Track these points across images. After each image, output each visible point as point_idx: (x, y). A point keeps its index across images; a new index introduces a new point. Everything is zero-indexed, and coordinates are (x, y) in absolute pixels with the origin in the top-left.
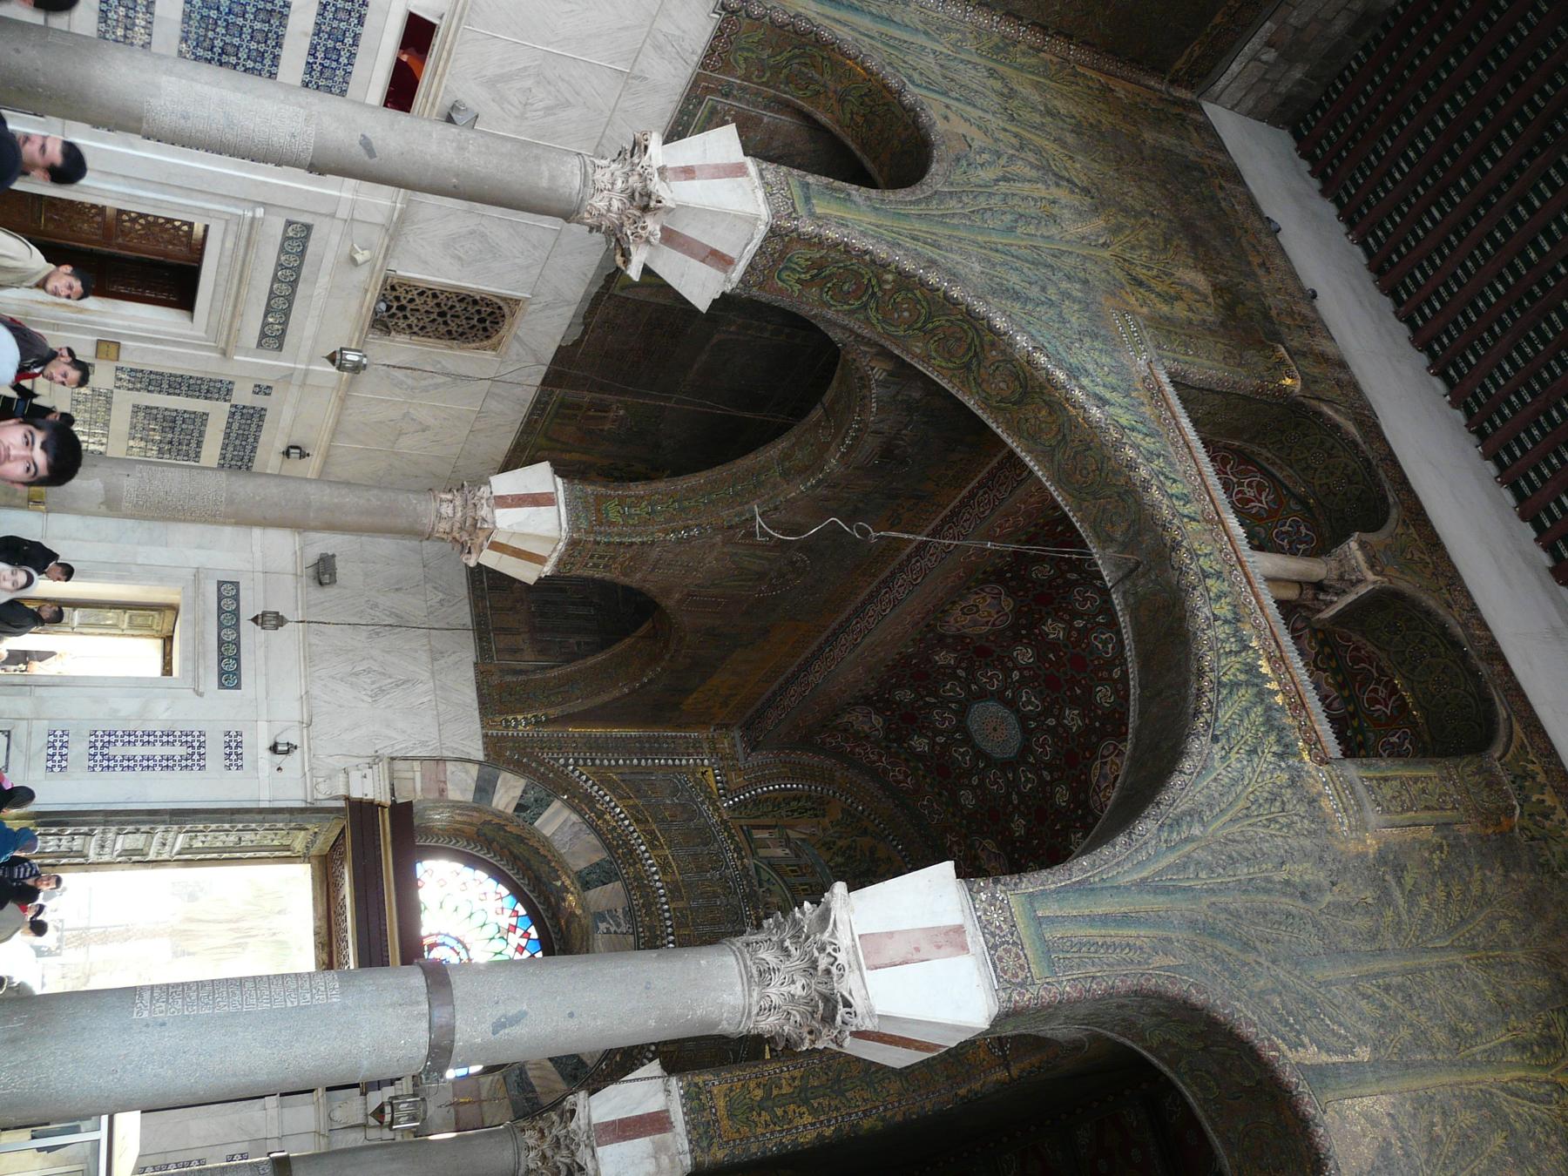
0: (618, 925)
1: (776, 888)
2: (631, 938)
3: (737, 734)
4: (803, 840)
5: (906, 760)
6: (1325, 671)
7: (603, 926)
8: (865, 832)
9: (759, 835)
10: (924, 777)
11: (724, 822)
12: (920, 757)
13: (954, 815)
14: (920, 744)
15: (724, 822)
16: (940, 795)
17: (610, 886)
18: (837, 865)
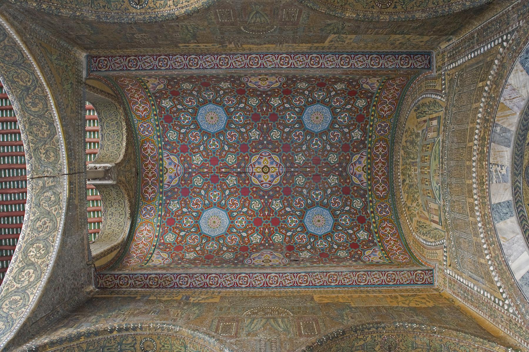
0: (496, 171)
1: (435, 184)
2: (491, 161)
3: (436, 284)
4: (424, 210)
5: (376, 233)
6: (165, 167)
7: (504, 172)
8: (409, 208)
9: (436, 218)
10: (374, 223)
11: (448, 231)
12: (368, 230)
13: (371, 201)
14: (363, 235)
15: (448, 231)
16: (372, 212)
17: (497, 202)
18: (416, 192)
